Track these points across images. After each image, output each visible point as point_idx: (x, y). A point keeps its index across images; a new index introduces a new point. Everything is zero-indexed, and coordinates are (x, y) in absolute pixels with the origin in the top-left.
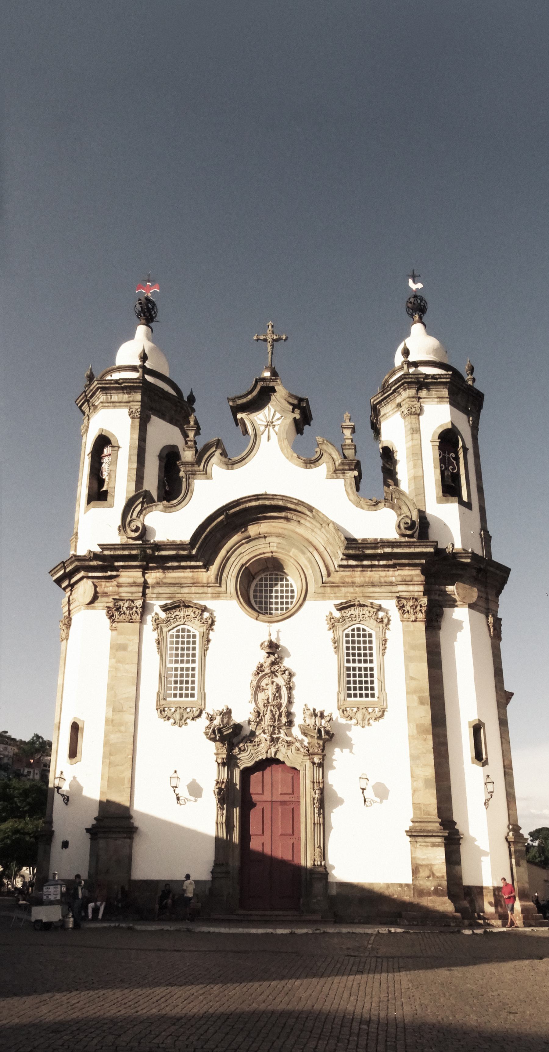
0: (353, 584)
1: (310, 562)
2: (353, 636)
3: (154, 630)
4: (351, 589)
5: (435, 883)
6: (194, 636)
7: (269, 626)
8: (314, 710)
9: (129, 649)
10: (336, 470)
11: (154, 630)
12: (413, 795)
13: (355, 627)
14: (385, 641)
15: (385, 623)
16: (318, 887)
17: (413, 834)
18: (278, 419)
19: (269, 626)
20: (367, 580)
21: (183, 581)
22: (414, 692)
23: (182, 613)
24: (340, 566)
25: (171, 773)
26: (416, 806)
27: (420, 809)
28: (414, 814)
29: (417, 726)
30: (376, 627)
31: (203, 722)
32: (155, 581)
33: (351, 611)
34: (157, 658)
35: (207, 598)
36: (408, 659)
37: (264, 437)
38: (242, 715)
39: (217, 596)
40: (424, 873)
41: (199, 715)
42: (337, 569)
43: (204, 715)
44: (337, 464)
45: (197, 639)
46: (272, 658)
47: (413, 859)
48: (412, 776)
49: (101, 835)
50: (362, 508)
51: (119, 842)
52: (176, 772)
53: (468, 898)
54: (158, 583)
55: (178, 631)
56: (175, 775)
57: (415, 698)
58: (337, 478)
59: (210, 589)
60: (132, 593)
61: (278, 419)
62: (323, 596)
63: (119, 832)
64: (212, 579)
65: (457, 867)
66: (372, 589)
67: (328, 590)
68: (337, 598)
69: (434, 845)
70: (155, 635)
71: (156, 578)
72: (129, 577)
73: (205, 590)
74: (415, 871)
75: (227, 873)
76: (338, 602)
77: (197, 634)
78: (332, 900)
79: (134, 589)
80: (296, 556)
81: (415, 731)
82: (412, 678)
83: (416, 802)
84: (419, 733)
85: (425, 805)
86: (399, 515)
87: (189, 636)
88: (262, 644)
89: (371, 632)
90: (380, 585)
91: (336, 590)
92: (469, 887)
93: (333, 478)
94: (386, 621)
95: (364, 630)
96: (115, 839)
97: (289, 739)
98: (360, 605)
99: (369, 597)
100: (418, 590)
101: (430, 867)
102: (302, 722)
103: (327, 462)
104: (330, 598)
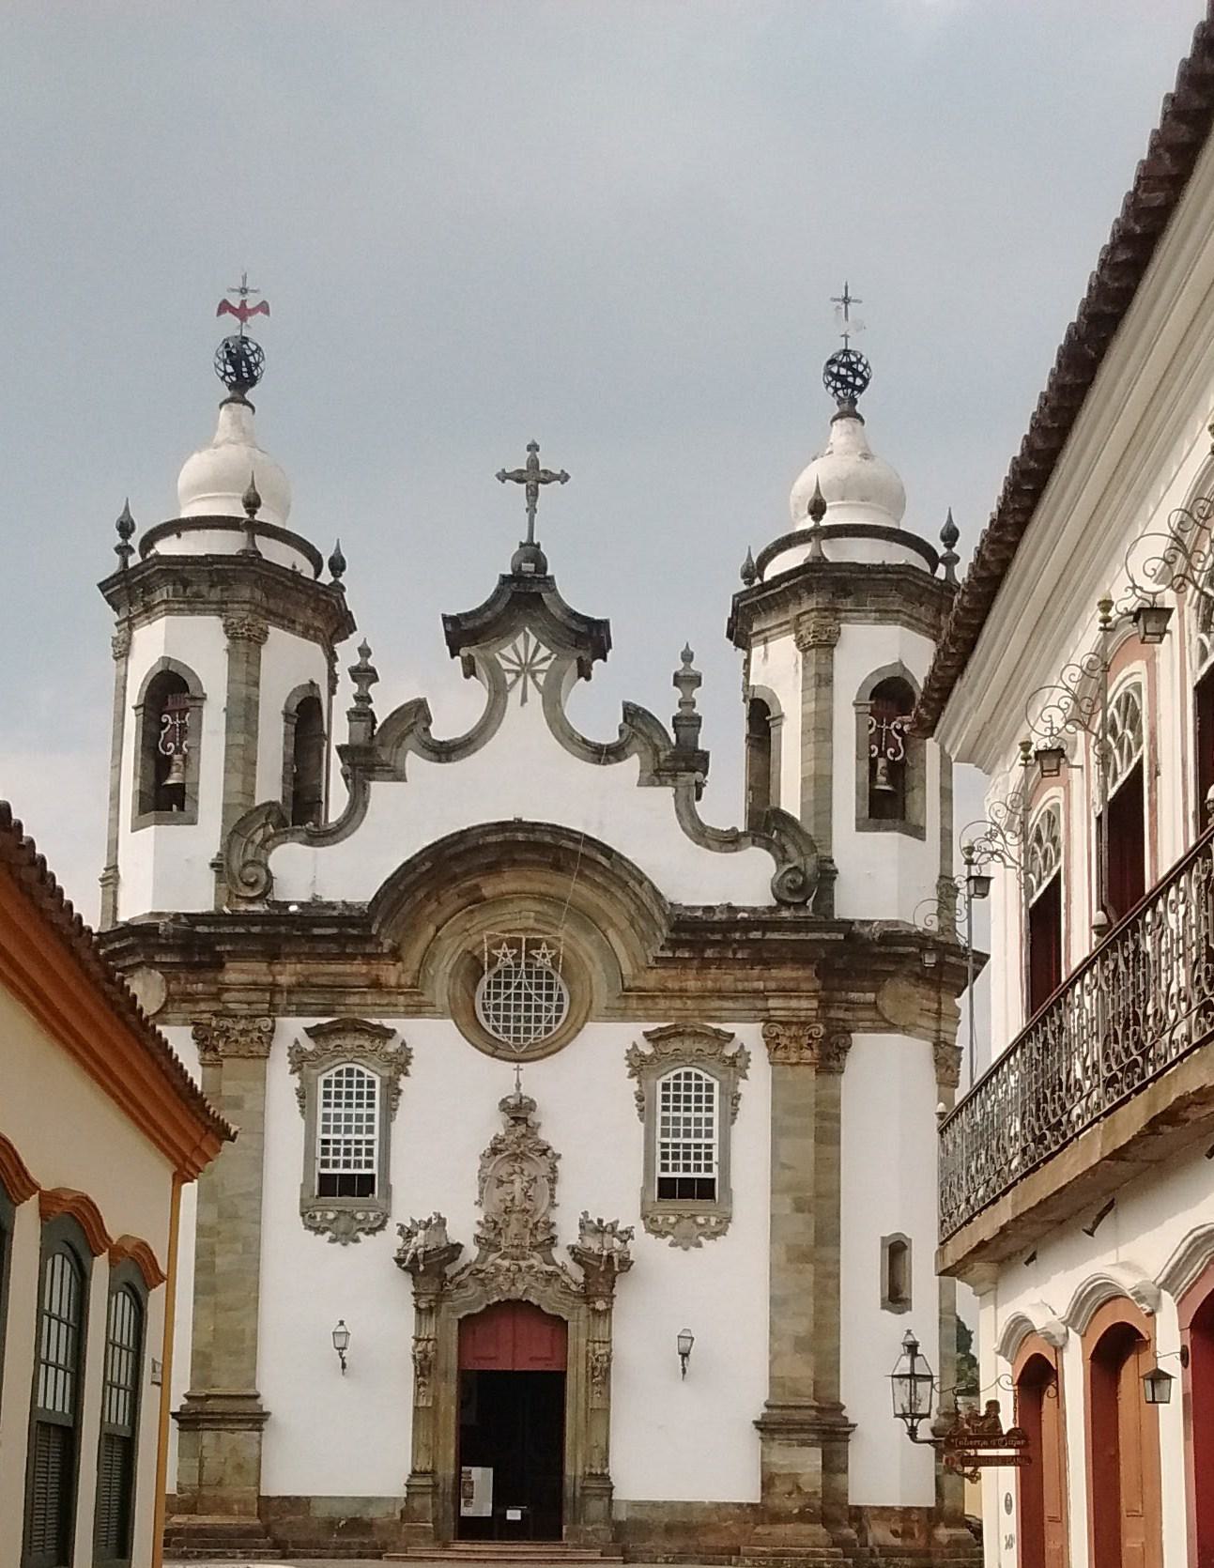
0: (682, 993)
1: (600, 946)
2: (677, 1087)
3: (293, 1072)
4: (678, 1003)
5: (801, 1503)
6: (371, 1084)
7: (518, 1069)
8: (600, 1221)
9: (247, 1106)
10: (656, 772)
11: (293, 1072)
12: (771, 1363)
13: (682, 1071)
14: (738, 1097)
15: (737, 1065)
16: (595, 1508)
17: (767, 1428)
18: (545, 659)
19: (518, 1069)
20: (710, 984)
21: (351, 981)
22: (789, 1189)
23: (349, 1042)
24: (657, 959)
25: (334, 1326)
26: (774, 1381)
27: (783, 1386)
28: (771, 1393)
29: (789, 1248)
30: (722, 1072)
31: (390, 1240)
32: (294, 979)
33: (674, 1045)
34: (300, 1123)
35: (396, 1015)
36: (778, 1131)
37: (514, 697)
38: (464, 1228)
39: (416, 1011)
40: (781, 1487)
41: (381, 1227)
42: (652, 963)
43: (392, 1227)
44: (662, 756)
45: (377, 1090)
46: (521, 1129)
47: (764, 1465)
48: (771, 1333)
49: (207, 1425)
50: (708, 847)
51: (240, 1436)
52: (342, 1323)
53: (856, 1525)
54: (299, 985)
55: (339, 1073)
56: (341, 1329)
57: (788, 1200)
58: (662, 784)
59: (401, 998)
60: (249, 1003)
61: (545, 659)
62: (622, 1015)
63: (240, 1421)
64: (406, 979)
65: (840, 1477)
66: (717, 1004)
67: (634, 1003)
68: (649, 1019)
69: (803, 1444)
70: (295, 1081)
71: (296, 974)
72: (243, 971)
73: (393, 999)
74: (767, 1483)
75: (436, 1486)
76: (652, 1027)
77: (377, 1080)
78: (619, 1529)
79: (254, 996)
80: (572, 937)
81: (784, 1258)
82: (784, 1166)
83: (778, 1374)
84: (789, 1260)
85: (793, 1380)
86: (782, 859)
87: (360, 1084)
88: (504, 1101)
89: (712, 1080)
90: (734, 995)
91: (649, 1003)
92: (858, 1508)
93: (653, 784)
94: (739, 1062)
95: (698, 1077)
96: (232, 1431)
97: (551, 1268)
98: (696, 1034)
99: (712, 1019)
100: (806, 1005)
101: (794, 1477)
102: (575, 1241)
103: (639, 753)
104: (635, 1019)
